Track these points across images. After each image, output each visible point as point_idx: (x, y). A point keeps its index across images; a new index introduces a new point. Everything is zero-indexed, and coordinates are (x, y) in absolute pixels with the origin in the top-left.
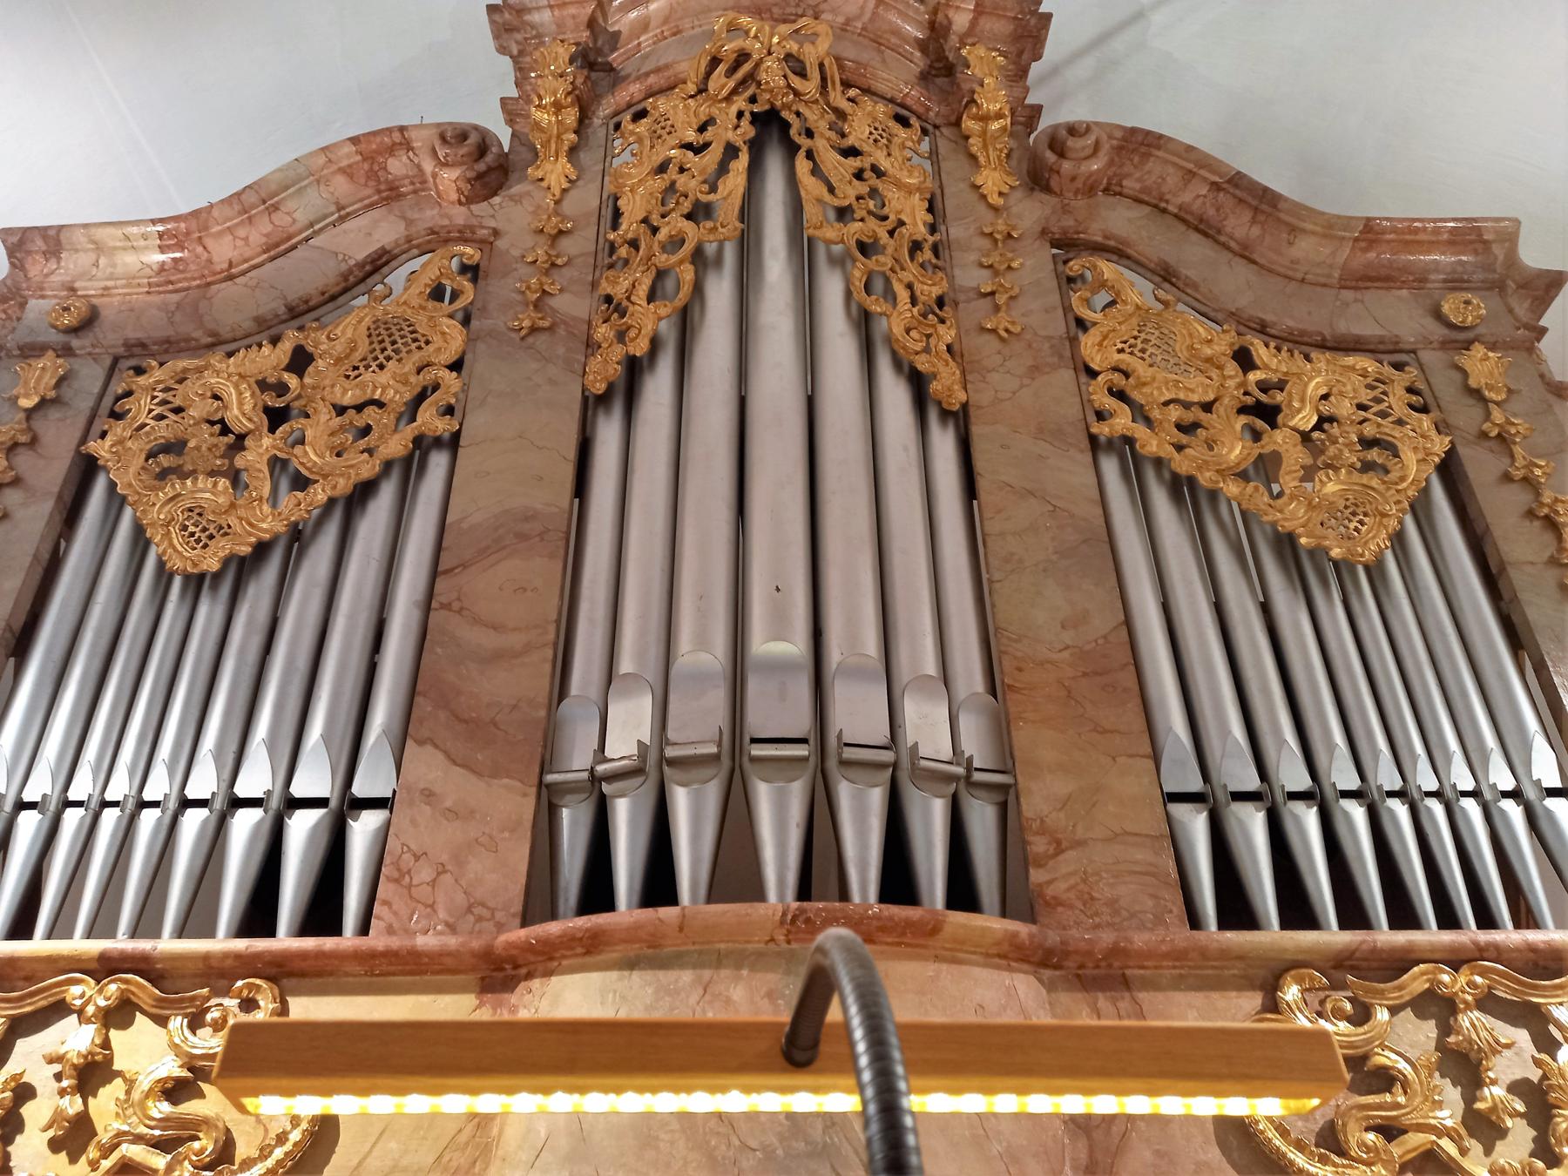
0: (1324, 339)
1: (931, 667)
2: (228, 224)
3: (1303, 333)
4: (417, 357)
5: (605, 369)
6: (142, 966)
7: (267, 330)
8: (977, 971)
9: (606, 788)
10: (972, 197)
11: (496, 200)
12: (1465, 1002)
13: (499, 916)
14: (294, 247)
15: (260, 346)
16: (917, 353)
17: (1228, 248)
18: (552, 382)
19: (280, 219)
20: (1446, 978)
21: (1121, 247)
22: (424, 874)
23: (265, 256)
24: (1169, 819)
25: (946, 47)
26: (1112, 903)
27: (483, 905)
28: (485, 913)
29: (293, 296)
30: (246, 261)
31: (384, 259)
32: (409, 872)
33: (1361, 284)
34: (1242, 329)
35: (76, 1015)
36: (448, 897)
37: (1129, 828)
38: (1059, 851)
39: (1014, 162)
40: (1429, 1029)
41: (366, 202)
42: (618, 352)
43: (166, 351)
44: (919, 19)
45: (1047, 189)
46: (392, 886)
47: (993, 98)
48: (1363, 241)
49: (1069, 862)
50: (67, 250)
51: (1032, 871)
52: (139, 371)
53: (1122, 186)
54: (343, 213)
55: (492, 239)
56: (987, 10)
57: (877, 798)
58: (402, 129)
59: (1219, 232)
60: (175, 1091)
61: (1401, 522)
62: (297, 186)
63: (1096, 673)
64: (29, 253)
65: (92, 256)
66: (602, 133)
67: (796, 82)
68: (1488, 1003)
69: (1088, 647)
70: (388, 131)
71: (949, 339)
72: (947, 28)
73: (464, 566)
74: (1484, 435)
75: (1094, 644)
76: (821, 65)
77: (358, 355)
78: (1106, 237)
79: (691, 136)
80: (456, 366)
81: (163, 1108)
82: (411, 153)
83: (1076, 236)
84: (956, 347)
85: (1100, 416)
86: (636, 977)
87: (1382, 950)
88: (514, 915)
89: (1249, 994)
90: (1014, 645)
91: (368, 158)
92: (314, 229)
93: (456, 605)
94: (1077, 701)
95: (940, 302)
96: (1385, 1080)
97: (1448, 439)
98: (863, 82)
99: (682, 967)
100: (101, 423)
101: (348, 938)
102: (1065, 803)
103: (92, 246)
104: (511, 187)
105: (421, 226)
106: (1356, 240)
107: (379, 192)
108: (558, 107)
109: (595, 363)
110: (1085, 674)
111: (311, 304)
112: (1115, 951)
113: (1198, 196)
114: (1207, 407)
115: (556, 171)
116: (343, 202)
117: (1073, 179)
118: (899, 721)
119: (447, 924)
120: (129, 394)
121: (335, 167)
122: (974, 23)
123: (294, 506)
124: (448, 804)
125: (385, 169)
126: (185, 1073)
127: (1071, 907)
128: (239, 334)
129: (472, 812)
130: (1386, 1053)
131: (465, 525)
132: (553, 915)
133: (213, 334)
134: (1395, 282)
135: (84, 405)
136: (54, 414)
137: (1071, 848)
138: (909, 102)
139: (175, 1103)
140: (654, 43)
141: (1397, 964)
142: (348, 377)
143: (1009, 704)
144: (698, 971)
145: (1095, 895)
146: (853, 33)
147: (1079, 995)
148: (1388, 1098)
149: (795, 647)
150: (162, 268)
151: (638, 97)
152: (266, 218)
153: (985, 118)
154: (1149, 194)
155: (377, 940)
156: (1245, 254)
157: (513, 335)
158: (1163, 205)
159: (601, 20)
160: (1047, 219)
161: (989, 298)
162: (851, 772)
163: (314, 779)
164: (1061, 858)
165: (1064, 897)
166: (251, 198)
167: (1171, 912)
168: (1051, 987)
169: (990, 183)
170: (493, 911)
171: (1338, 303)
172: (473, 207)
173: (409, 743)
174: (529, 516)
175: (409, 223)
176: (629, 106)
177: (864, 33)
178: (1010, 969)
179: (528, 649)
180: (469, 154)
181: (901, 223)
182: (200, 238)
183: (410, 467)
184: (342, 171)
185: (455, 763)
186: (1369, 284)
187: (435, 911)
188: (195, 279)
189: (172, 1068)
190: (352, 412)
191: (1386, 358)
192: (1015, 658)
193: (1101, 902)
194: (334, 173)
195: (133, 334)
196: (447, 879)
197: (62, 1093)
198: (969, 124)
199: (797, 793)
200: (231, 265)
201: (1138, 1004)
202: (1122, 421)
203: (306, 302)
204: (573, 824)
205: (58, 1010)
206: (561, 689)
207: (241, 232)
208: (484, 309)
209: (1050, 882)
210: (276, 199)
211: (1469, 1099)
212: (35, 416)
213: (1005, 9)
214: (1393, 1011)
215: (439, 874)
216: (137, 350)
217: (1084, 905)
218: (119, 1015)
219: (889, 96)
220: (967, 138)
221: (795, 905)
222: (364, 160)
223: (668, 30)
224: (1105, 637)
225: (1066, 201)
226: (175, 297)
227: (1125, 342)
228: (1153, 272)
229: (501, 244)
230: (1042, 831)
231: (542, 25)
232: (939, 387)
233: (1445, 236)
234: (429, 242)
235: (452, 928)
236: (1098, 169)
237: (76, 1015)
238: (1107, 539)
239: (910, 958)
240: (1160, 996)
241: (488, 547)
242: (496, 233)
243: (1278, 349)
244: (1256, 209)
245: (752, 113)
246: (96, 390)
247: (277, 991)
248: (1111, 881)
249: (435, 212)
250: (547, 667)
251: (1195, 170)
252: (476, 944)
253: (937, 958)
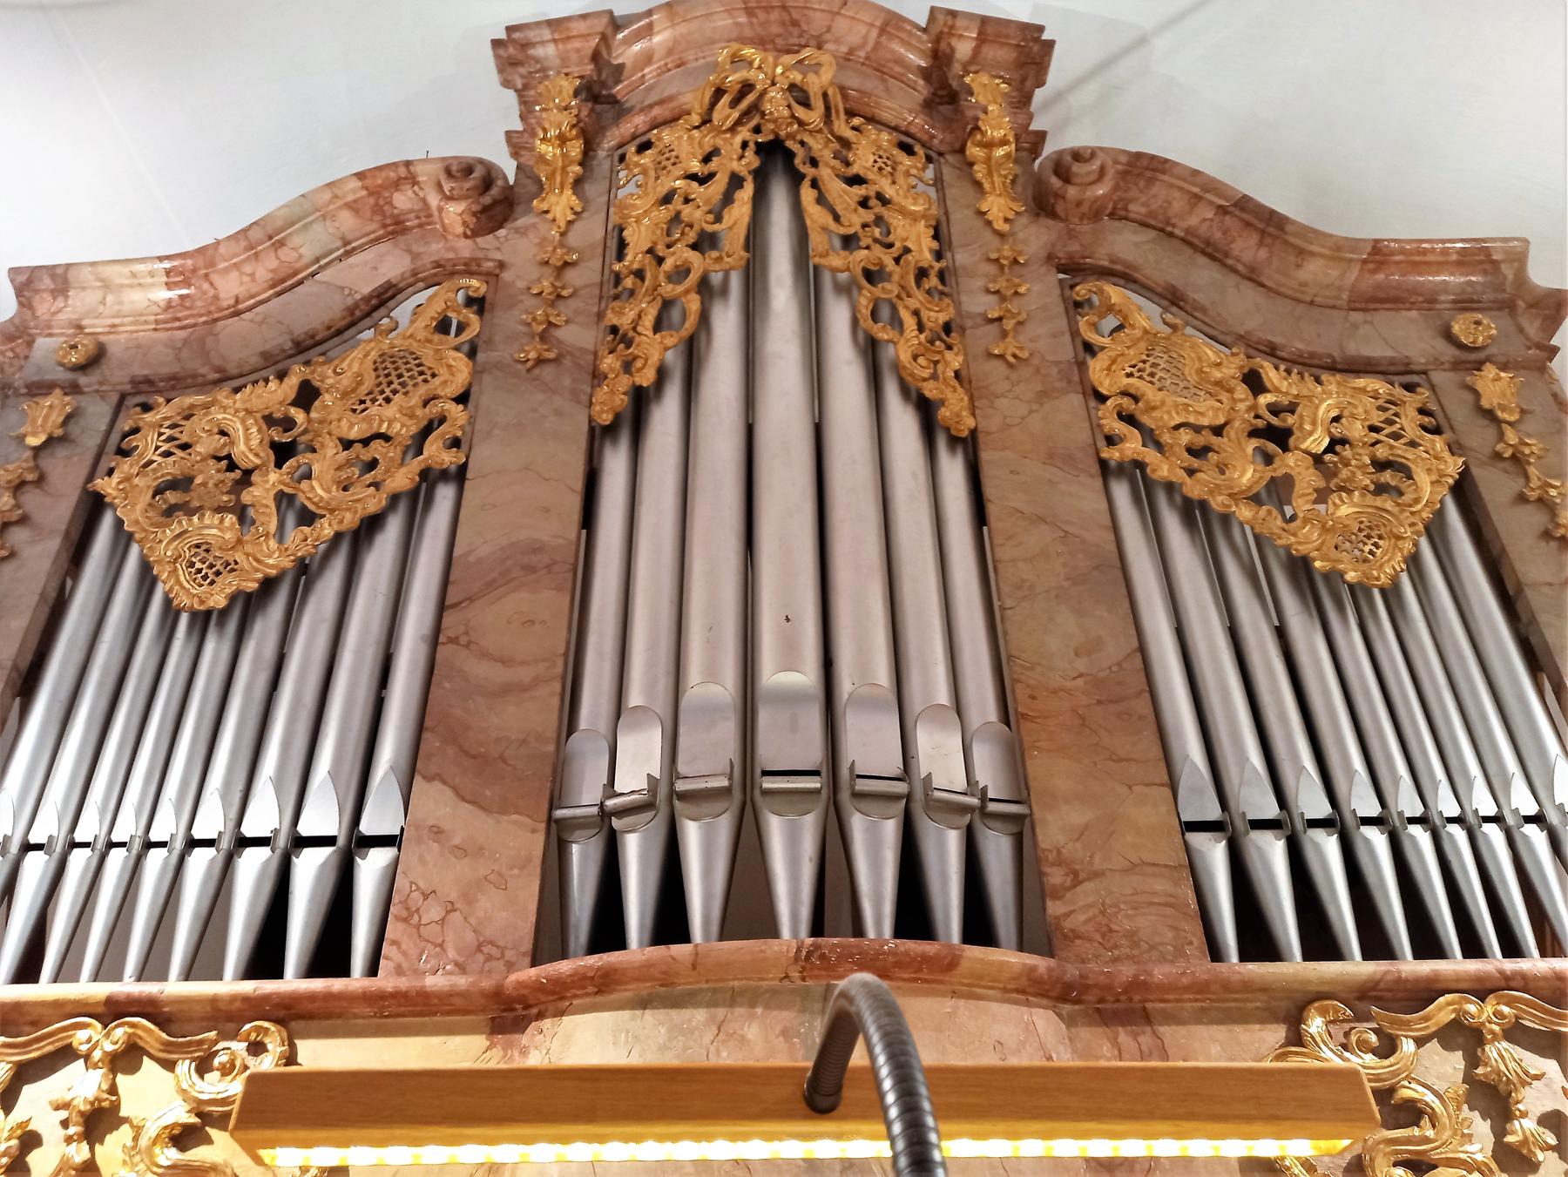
0: (1334, 361)
1: (943, 696)
2: (235, 261)
3: (1312, 355)
4: (423, 390)
5: (611, 400)
6: (149, 1009)
7: (274, 364)
8: (994, 1006)
10: (979, 223)
11: (502, 232)
12: (1492, 1032)
13: (509, 955)
14: (300, 283)
15: (267, 381)
16: (925, 380)
17: (1235, 271)
18: (559, 413)
19: (287, 254)
20: (1472, 1008)
21: (1127, 271)
22: (433, 912)
23: (271, 292)
24: (1187, 847)
25: (950, 75)
26: (1131, 935)
27: (492, 943)
28: (494, 952)
29: (301, 328)
30: (252, 297)
31: (390, 293)
32: (418, 910)
33: (1372, 306)
34: (1252, 352)
35: (82, 1061)
36: (458, 936)
37: (1147, 858)
38: (1077, 882)
39: (1019, 188)
40: (1457, 1060)
41: (372, 236)
42: (624, 383)
43: (173, 388)
44: (922, 47)
45: (1053, 215)
46: (401, 926)
47: (998, 124)
48: (1371, 262)
49: (1087, 894)
50: (75, 288)
51: (1049, 903)
52: (147, 408)
53: (1127, 210)
54: (349, 248)
55: (497, 271)
56: (989, 38)
57: (890, 830)
58: (408, 164)
59: (1226, 255)
60: (183, 1137)
61: (1416, 544)
62: (303, 222)
63: (1111, 701)
64: (37, 291)
65: (99, 295)
66: (606, 165)
67: (800, 112)
68: (1516, 1033)
69: (1103, 674)
70: (394, 166)
71: (956, 365)
73: (471, 599)
74: (1497, 456)
75: (1108, 671)
76: (825, 95)
77: (364, 389)
78: (1112, 261)
79: (695, 166)
80: (462, 399)
81: (170, 1155)
82: (416, 188)
83: (1082, 261)
84: (964, 373)
85: (1111, 440)
87: (1407, 981)
88: (524, 954)
89: (1274, 1026)
90: (1027, 673)
91: (374, 192)
92: (320, 264)
93: (463, 640)
94: (1091, 729)
95: (947, 328)
96: (1412, 1113)
97: (1461, 461)
98: (868, 111)
99: (696, 1005)
100: (108, 461)
101: (356, 980)
102: (1082, 832)
103: (99, 284)
104: (516, 220)
105: (427, 260)
106: (1364, 262)
107: (385, 226)
108: (562, 140)
110: (1099, 702)
111: (317, 338)
112: (1135, 985)
113: (1205, 220)
114: (1218, 431)
115: (561, 203)
116: (349, 237)
117: (1079, 204)
118: (912, 752)
119: (456, 964)
120: (136, 431)
121: (340, 203)
122: (976, 51)
123: (301, 541)
124: (457, 841)
125: (390, 203)
126: (194, 1120)
127: (1090, 940)
128: (246, 369)
129: (482, 848)
130: (1413, 1085)
131: (471, 559)
132: (564, 955)
133: (219, 370)
134: (1403, 303)
135: (91, 442)
136: (61, 452)
137: (1089, 879)
138: (913, 130)
139: (183, 1149)
140: (659, 75)
141: (1422, 995)
142: (354, 411)
143: (1024, 733)
144: (713, 1010)
145: (1115, 927)
146: (857, 62)
147: (1100, 1030)
148: (1416, 1131)
149: (806, 677)
150: (169, 305)
151: (642, 128)
152: (272, 254)
153: (989, 145)
154: (1155, 218)
155: (386, 981)
156: (1252, 276)
157: (519, 366)
158: (1169, 229)
159: (605, 54)
160: (1053, 245)
161: (996, 324)
162: (864, 805)
163: (322, 817)
164: (1078, 889)
165: (1082, 929)
166: (256, 234)
167: (1191, 943)
168: (1070, 1022)
169: (995, 210)
170: (503, 949)
171: (1347, 325)
172: (479, 240)
173: (418, 780)
174: (538, 548)
175: (415, 256)
176: (634, 137)
177: (867, 62)
178: (1028, 1004)
179: (536, 682)
180: (475, 188)
181: (907, 250)
182: (206, 275)
183: (416, 501)
184: (348, 206)
185: (463, 799)
186: (1379, 306)
187: (444, 950)
188: (201, 315)
189: (183, 1115)
190: (358, 446)
191: (1398, 379)
192: (1028, 686)
193: (1121, 934)
194: (341, 208)
195: (140, 371)
196: (456, 917)
197: (69, 1140)
198: (974, 151)
199: (809, 824)
200: (237, 301)
201: (1159, 1038)
202: (1133, 446)
203: (312, 337)
204: (583, 859)
205: (65, 1055)
207: (248, 269)
208: (490, 342)
209: (1068, 915)
210: (282, 235)
211: (1499, 1132)
212: (43, 454)
213: (1007, 37)
214: (1420, 1042)
215: (448, 912)
216: (144, 387)
217: (1103, 938)
218: (126, 1059)
219: (893, 124)
220: (971, 164)
221: (810, 941)
222: (371, 194)
223: (672, 62)
224: (1119, 664)
225: (1071, 226)
226: (182, 334)
227: (1134, 366)
228: (1161, 296)
229: (506, 276)
230: (1060, 862)
231: (546, 58)
232: (948, 414)
233: (1454, 257)
234: (435, 275)
235: (461, 968)
236: (1104, 196)
237: (82, 1061)
238: (1119, 565)
239: (927, 994)
240: (1182, 1030)
241: (494, 581)
242: (502, 265)
243: (1288, 372)
244: (1263, 233)
245: (757, 144)
246: (103, 428)
247: (285, 1034)
248: (1130, 912)
249: (441, 245)
250: (556, 701)
251: (1201, 194)
252: (487, 984)
253: (954, 994)
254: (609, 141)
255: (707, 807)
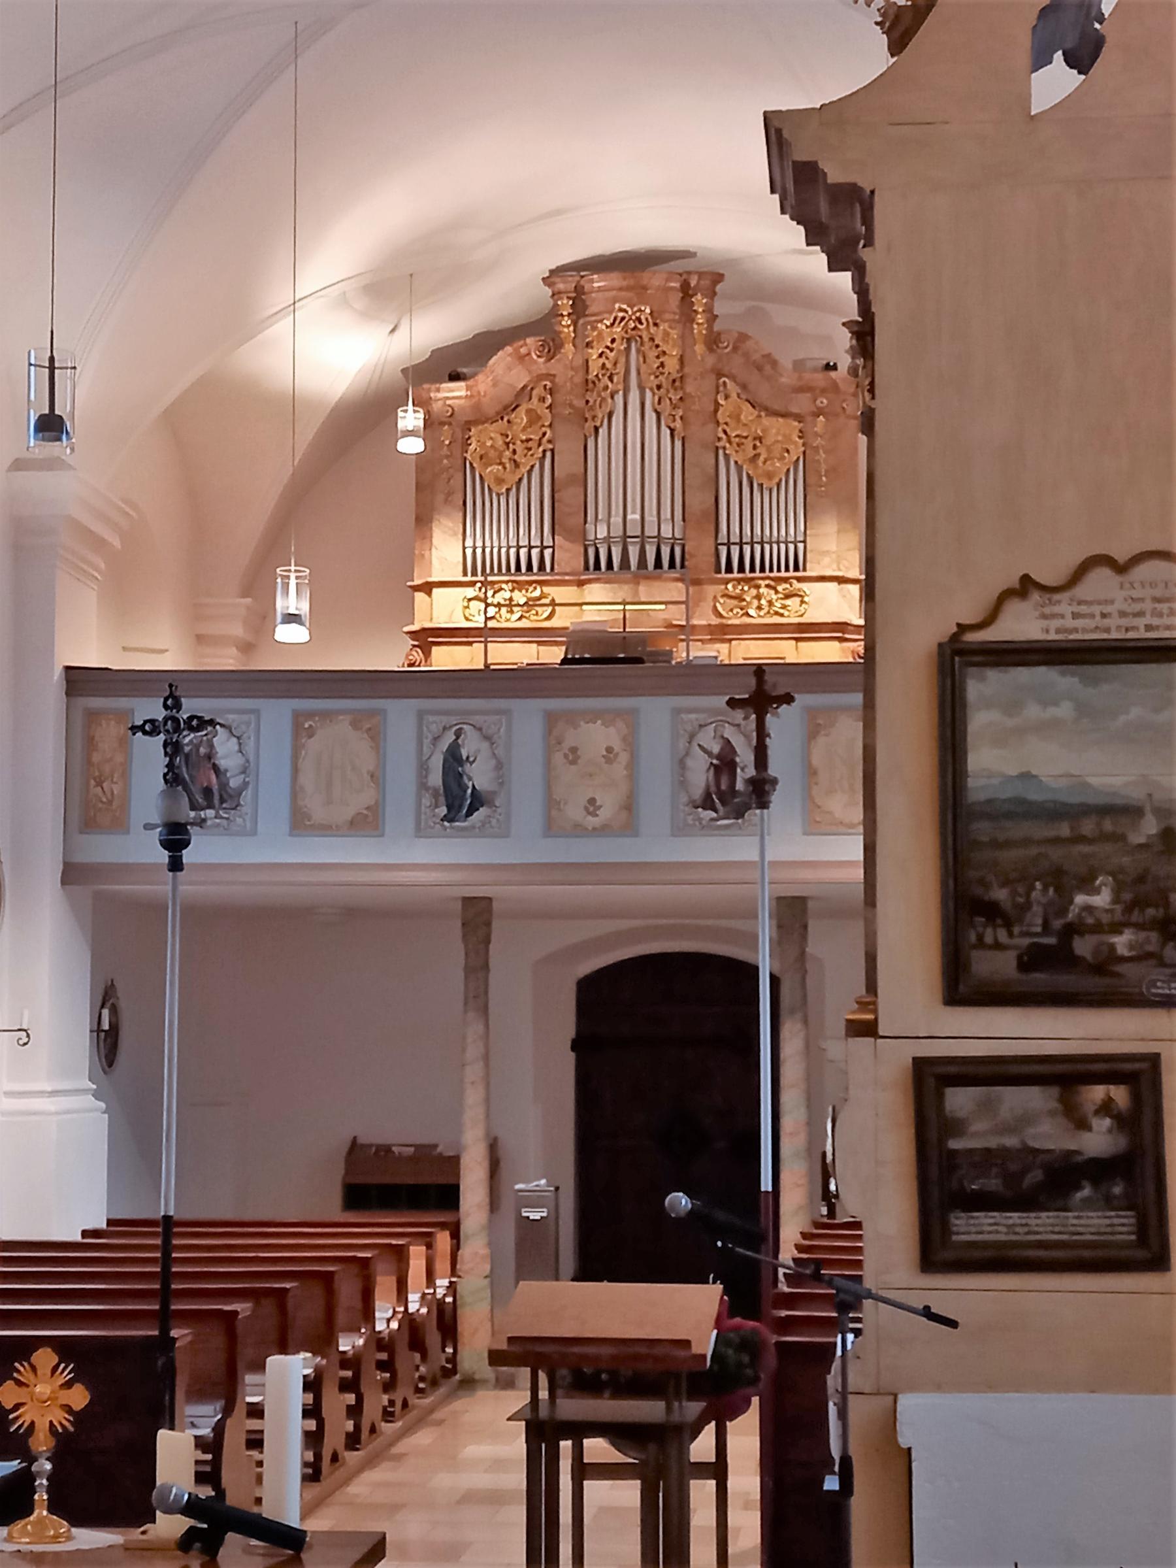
1: (669, 516)
4: (540, 424)
5: (589, 425)
9: (598, 546)
11: (553, 361)
42: (593, 424)
47: (700, 319)
68: (767, 586)
71: (681, 414)
72: (689, 284)
85: (719, 439)
86: (607, 585)
95: (681, 398)
109: (587, 425)
114: (746, 437)
115: (569, 348)
120: (469, 438)
149: (637, 517)
163: (536, 542)
173: (556, 537)
175: (530, 372)
184: (509, 355)
199: (638, 547)
204: (591, 552)
205: (502, 589)
206: (585, 522)
214: (749, 588)
218: (512, 591)
229: (557, 380)
242: (554, 376)
254: (581, 321)
255: (617, 544)
